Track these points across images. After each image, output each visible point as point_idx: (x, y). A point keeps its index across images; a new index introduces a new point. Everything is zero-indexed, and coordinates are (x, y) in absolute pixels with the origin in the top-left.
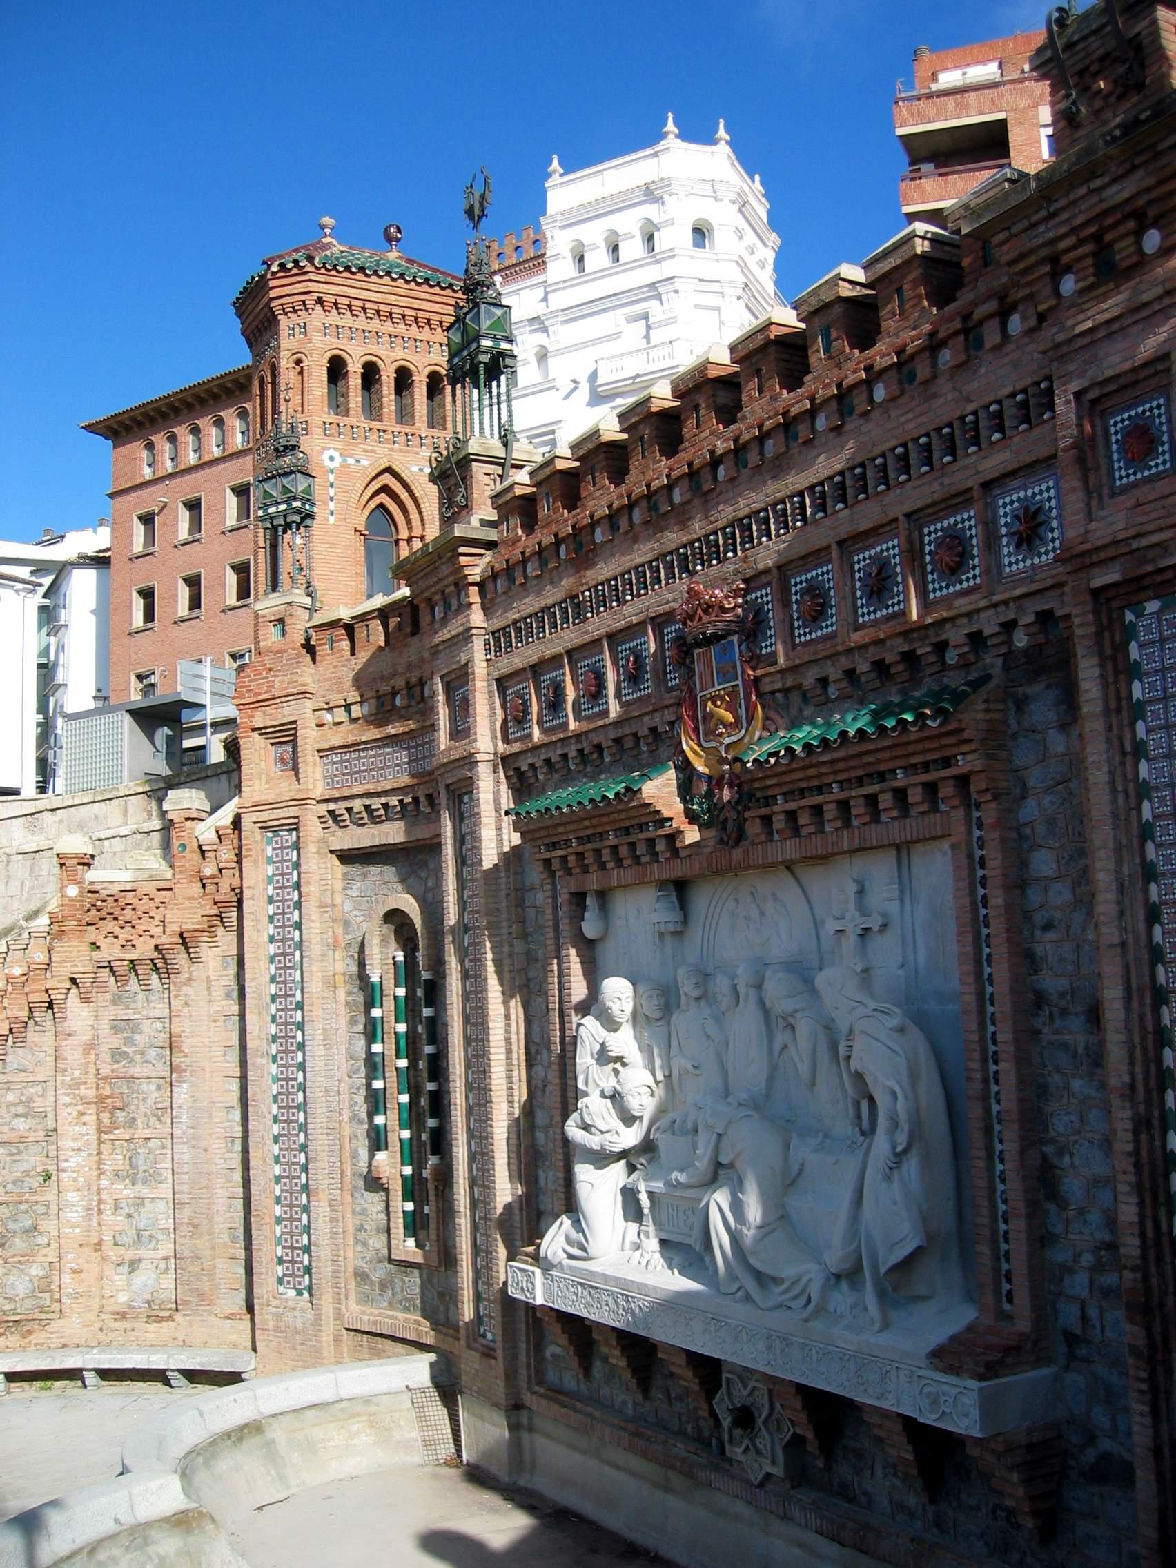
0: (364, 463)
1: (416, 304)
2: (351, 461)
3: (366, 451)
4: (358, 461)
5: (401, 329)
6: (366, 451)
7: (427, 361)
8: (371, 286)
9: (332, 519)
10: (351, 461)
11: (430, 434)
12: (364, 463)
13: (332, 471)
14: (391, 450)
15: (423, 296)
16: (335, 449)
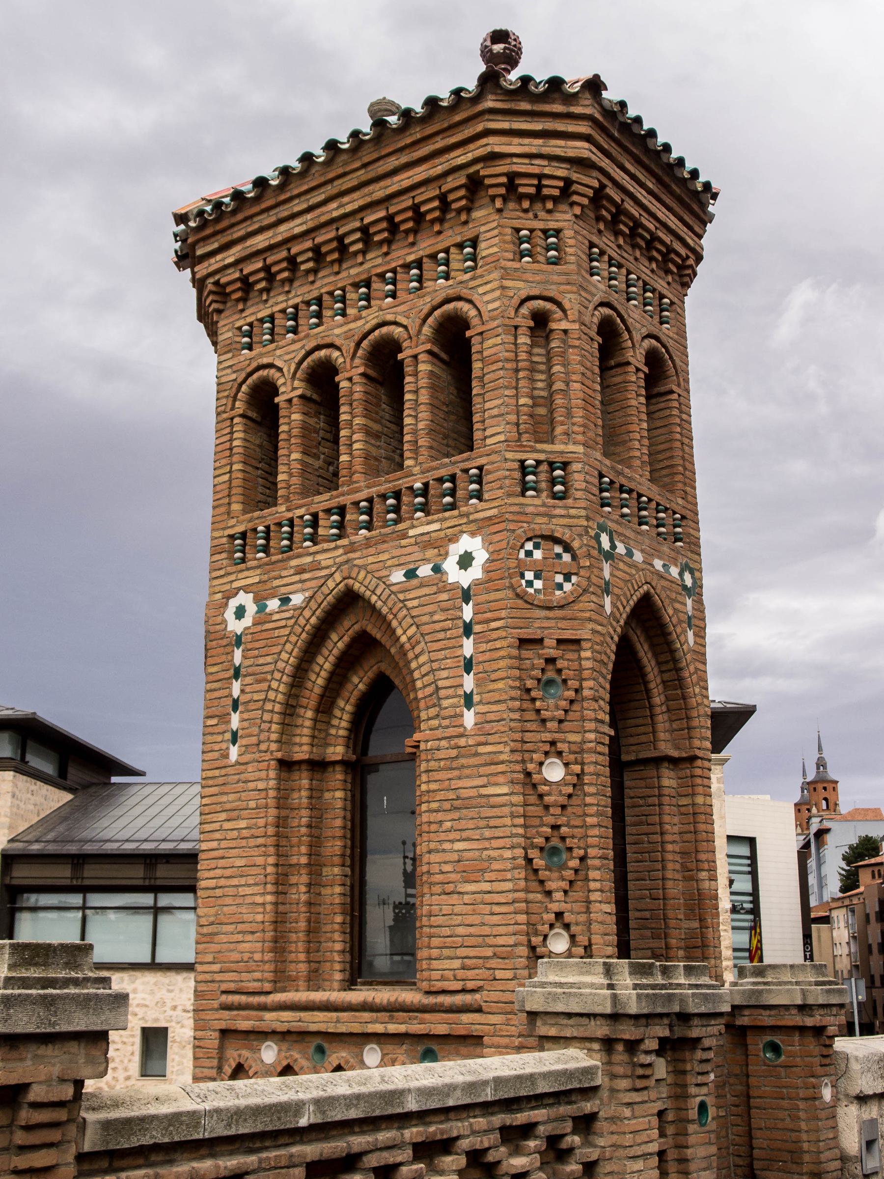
0: (297, 599)
1: (379, 191)
2: (273, 604)
3: (301, 570)
4: (285, 600)
5: (375, 262)
6: (301, 570)
7: (425, 303)
8: (298, 206)
9: (234, 752)
10: (273, 604)
11: (430, 476)
12: (297, 599)
13: (238, 641)
14: (352, 548)
15: (393, 162)
16: (246, 589)
